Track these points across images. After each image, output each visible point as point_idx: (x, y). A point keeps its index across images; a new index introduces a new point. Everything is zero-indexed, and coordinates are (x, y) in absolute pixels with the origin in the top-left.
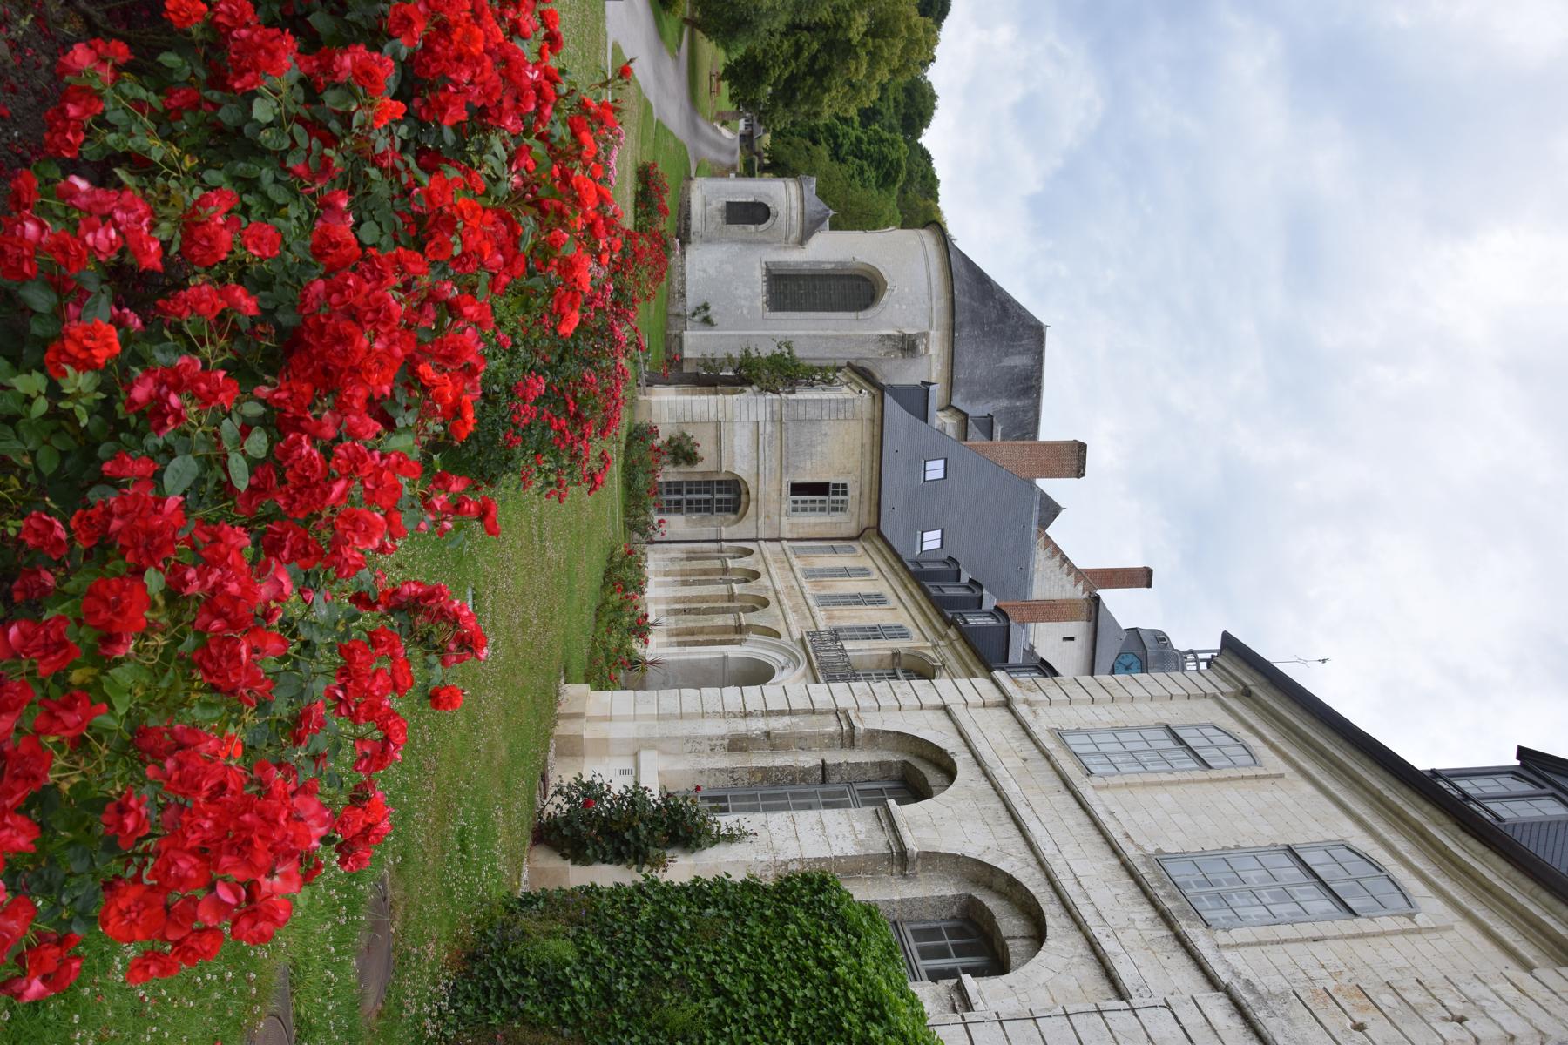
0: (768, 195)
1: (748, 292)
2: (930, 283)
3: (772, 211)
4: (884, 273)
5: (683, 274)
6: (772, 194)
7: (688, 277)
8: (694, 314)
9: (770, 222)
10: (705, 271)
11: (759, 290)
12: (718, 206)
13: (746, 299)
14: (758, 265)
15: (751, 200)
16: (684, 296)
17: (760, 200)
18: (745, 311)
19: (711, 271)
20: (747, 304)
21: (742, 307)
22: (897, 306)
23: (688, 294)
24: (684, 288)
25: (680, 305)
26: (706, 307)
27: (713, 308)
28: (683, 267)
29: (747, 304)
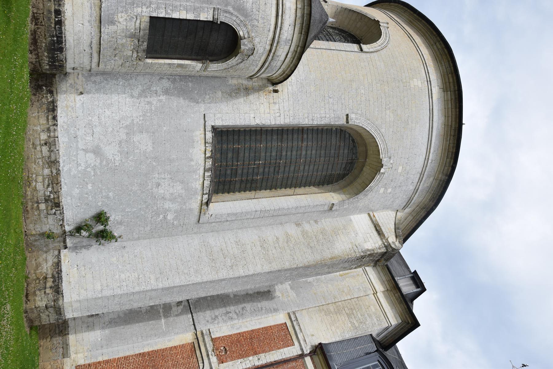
1: (178, 189)
2: (427, 159)
3: (245, 46)
4: (381, 147)
5: (53, 163)
7: (64, 167)
8: (79, 229)
9: (233, 61)
10: (97, 151)
11: (198, 185)
12: (132, 26)
13: (173, 200)
14: (199, 134)
15: (206, 16)
16: (57, 205)
17: (223, 18)
18: (170, 217)
20: (174, 206)
21: (166, 211)
23: (65, 201)
24: (57, 193)
25: (51, 219)
26: (100, 218)
27: (114, 217)
28: (51, 144)
29: (174, 206)
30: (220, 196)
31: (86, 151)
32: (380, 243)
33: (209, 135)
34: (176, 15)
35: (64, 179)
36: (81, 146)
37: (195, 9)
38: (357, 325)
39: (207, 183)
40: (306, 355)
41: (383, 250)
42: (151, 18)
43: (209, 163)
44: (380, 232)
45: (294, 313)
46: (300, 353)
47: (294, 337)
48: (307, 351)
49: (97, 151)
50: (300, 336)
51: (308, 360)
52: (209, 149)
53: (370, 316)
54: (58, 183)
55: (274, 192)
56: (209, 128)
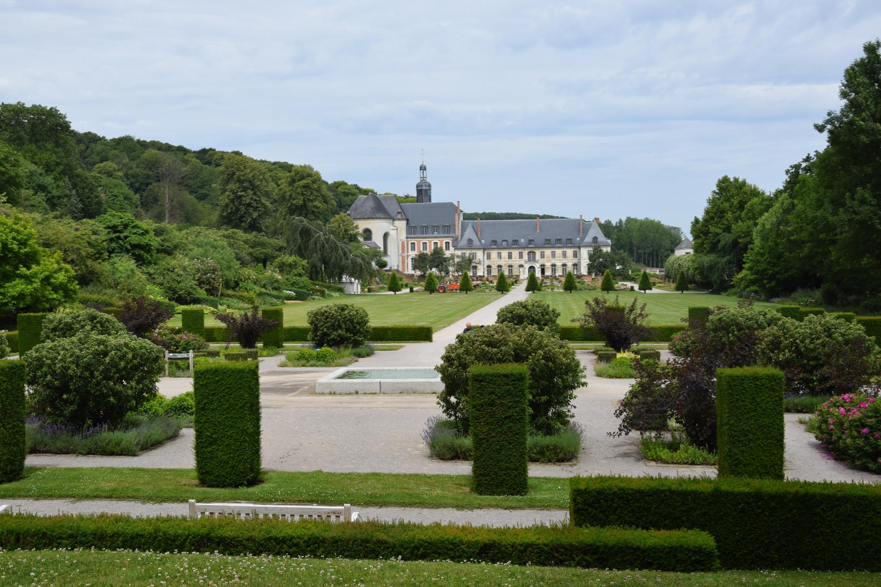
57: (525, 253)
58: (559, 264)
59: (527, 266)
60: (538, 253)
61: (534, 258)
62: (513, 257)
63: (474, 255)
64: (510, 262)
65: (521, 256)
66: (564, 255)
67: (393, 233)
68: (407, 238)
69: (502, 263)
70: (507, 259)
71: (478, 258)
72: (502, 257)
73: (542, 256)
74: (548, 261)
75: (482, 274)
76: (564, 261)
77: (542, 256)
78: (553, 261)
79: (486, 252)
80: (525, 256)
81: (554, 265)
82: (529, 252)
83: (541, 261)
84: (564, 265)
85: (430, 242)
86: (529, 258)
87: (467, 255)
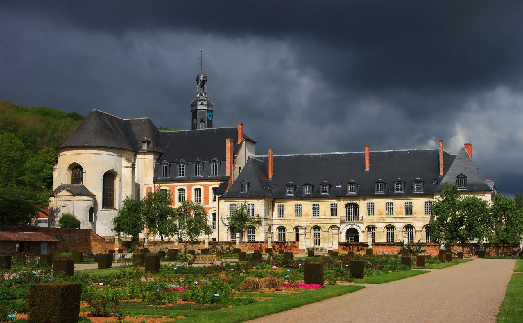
0: (87, 207)
6: (86, 206)
14: (104, 212)
15: (89, 213)
19: (106, 227)
22: (117, 167)
30: (114, 206)
31: (106, 231)
32: (129, 168)
33: (104, 210)
34: (89, 218)
35: (110, 235)
36: (105, 232)
37: (88, 215)
38: (151, 168)
39: (112, 210)
40: (155, 185)
41: (131, 168)
42: (90, 221)
43: (109, 210)
44: (127, 167)
45: (144, 185)
46: (154, 187)
47: (150, 187)
48: (153, 184)
49: (106, 230)
50: (150, 185)
51: (156, 185)
52: (106, 210)
53: (150, 163)
54: (110, 236)
55: (115, 194)
56: (103, 210)
57: (341, 205)
58: (399, 225)
59: (344, 229)
60: (363, 205)
61: (357, 214)
62: (321, 212)
63: (251, 209)
64: (316, 221)
65: (334, 211)
66: (409, 210)
67: (125, 173)
68: (155, 181)
69: (303, 222)
70: (311, 217)
71: (256, 212)
72: (303, 213)
73: (371, 210)
74: (380, 220)
75: (263, 239)
76: (409, 220)
77: (371, 210)
78: (390, 220)
79: (276, 204)
80: (342, 212)
81: (390, 228)
82: (347, 205)
83: (369, 220)
84: (409, 227)
85: (189, 188)
86: (348, 214)
87: (239, 207)
